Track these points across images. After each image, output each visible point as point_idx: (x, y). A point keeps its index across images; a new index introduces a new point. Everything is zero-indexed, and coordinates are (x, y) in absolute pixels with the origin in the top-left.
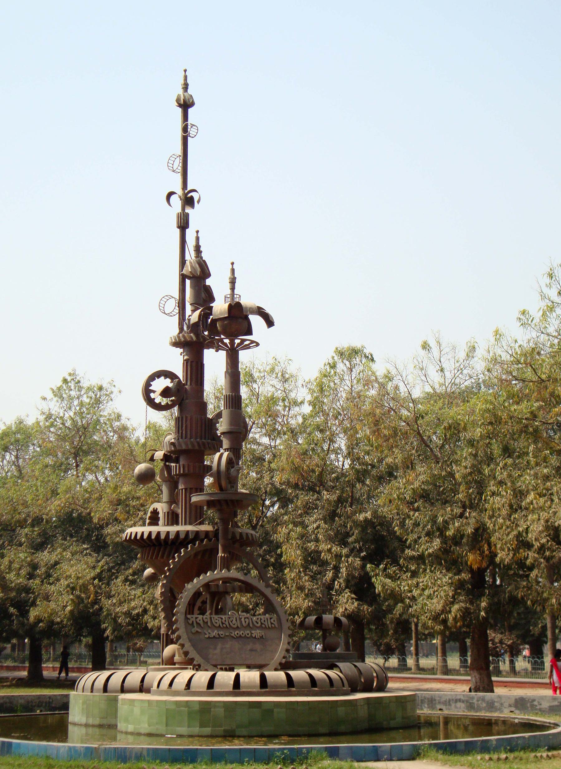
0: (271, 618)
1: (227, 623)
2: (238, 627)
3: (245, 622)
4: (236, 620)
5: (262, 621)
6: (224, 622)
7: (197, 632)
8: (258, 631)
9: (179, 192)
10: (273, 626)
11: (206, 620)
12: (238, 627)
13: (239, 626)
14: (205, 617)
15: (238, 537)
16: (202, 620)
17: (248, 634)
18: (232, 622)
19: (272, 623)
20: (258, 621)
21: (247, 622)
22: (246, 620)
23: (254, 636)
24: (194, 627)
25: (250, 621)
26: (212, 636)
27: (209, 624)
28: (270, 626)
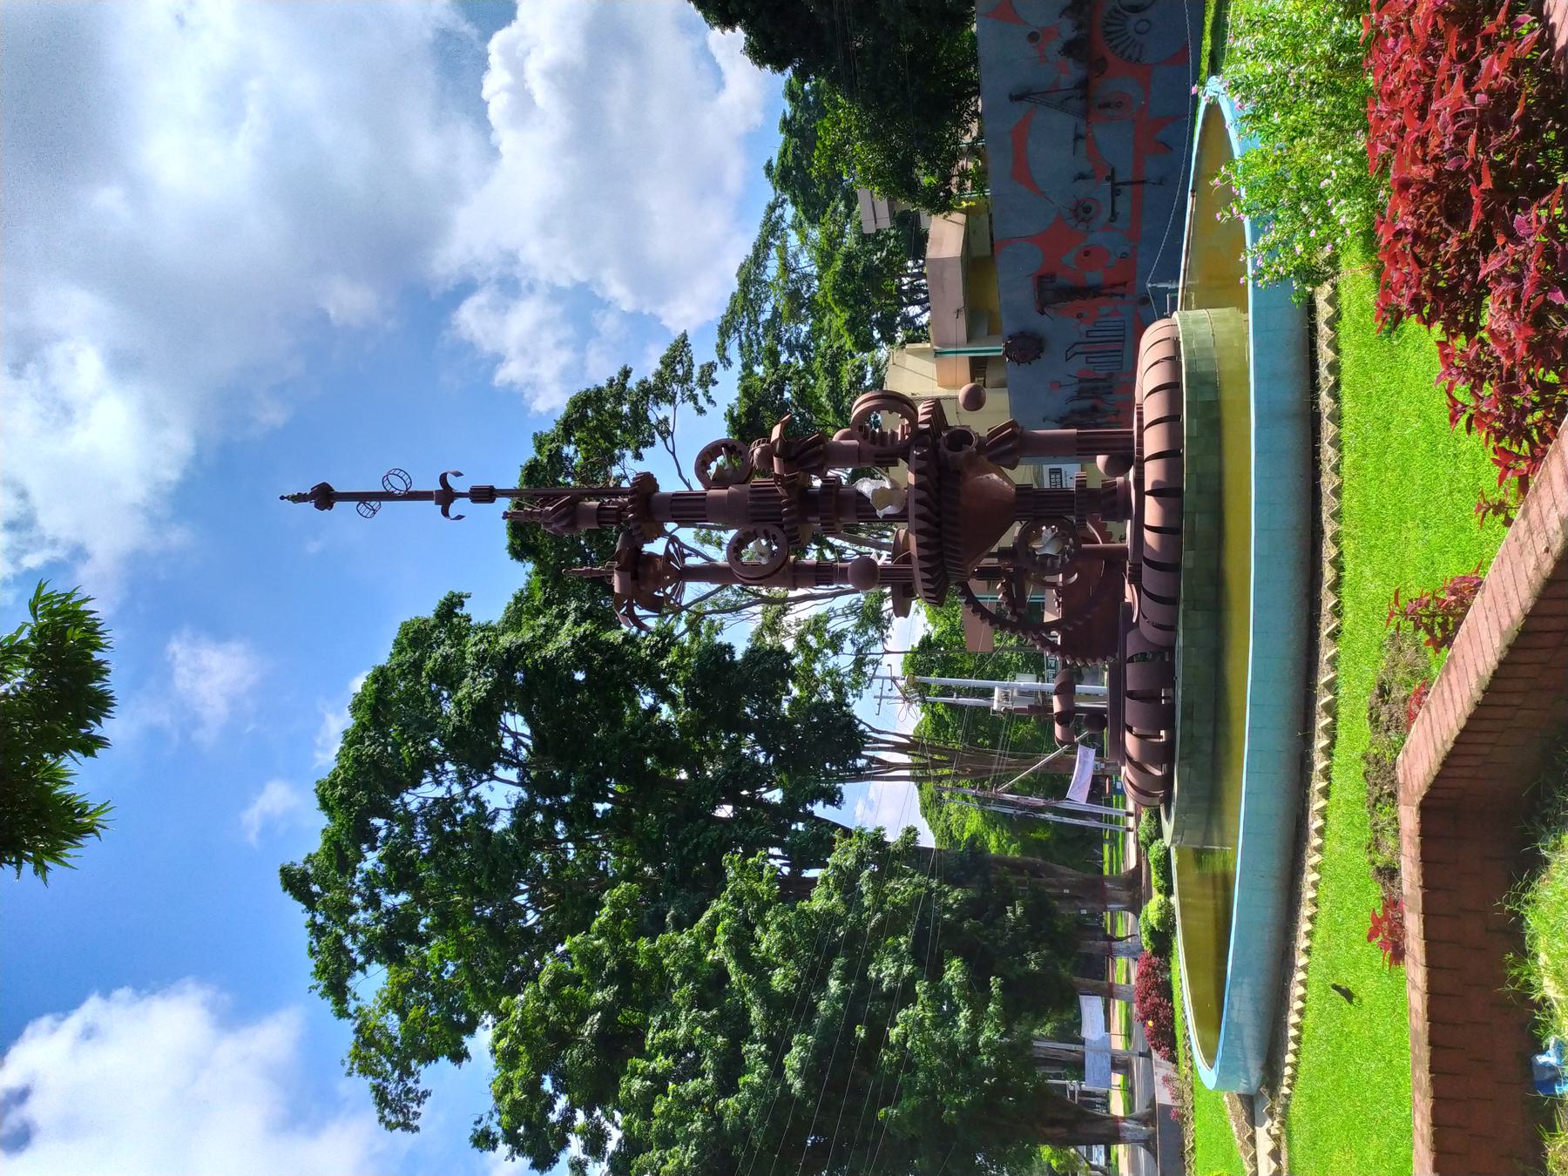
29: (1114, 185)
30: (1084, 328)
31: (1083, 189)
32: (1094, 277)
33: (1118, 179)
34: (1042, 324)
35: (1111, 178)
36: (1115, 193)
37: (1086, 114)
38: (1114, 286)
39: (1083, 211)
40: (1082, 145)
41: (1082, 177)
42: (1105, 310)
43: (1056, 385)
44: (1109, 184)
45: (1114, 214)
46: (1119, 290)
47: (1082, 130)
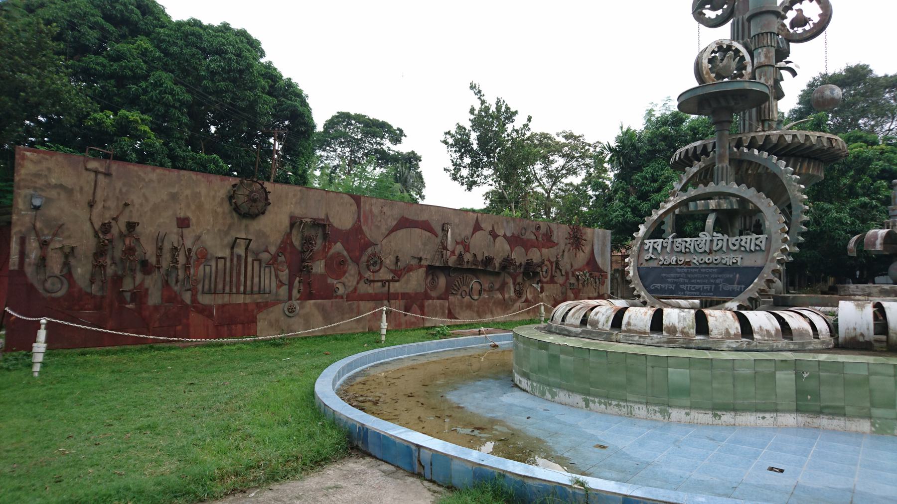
0: (757, 239)
1: (692, 248)
2: (705, 251)
3: (718, 244)
4: (705, 244)
5: (743, 243)
6: (687, 246)
7: (651, 258)
8: (732, 256)
10: (757, 248)
11: (665, 245)
12: (705, 251)
13: (708, 251)
14: (666, 240)
16: (660, 246)
17: (716, 260)
18: (698, 245)
19: (756, 245)
20: (737, 243)
21: (720, 246)
22: (720, 243)
23: (724, 262)
24: (649, 253)
25: (725, 244)
26: (668, 263)
27: (668, 249)
28: (753, 249)
29: (388, 281)
30: (265, 256)
33: (391, 284)
40: (414, 262)
44: (391, 278)
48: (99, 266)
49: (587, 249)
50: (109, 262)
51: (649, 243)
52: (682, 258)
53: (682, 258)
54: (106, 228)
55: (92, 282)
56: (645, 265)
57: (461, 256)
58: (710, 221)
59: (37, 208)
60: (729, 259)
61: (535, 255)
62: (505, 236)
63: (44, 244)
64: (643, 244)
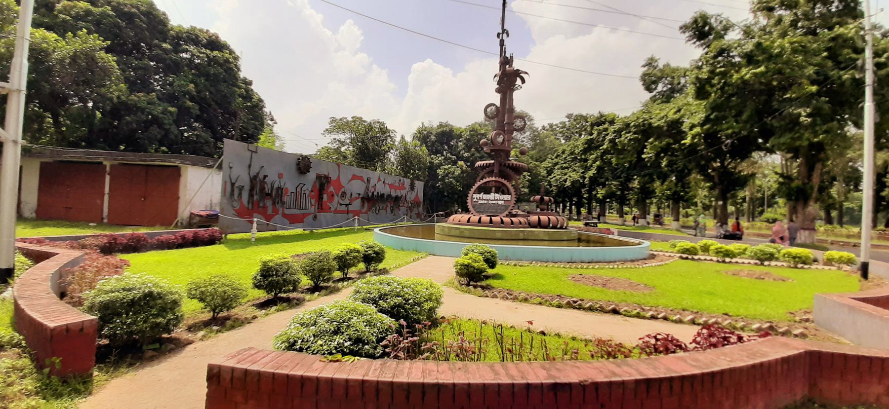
9: (501, 32)
15: (507, 165)
29: (348, 205)
30: (307, 192)
31: (348, 195)
32: (325, 197)
33: (349, 206)
34: (312, 176)
35: (350, 204)
36: (347, 205)
37: (362, 198)
38: (321, 205)
39: (344, 194)
40: (357, 196)
41: (351, 195)
42: (313, 201)
43: (280, 176)
45: (341, 204)
46: (320, 207)
47: (361, 196)
48: (251, 195)
49: (416, 191)
50: (255, 193)
51: (475, 196)
52: (486, 202)
53: (486, 202)
54: (256, 177)
55: (249, 203)
56: (474, 203)
57: (373, 193)
58: (494, 189)
59: (231, 168)
60: (500, 203)
61: (399, 193)
62: (388, 184)
63: (233, 184)
64: (472, 196)
